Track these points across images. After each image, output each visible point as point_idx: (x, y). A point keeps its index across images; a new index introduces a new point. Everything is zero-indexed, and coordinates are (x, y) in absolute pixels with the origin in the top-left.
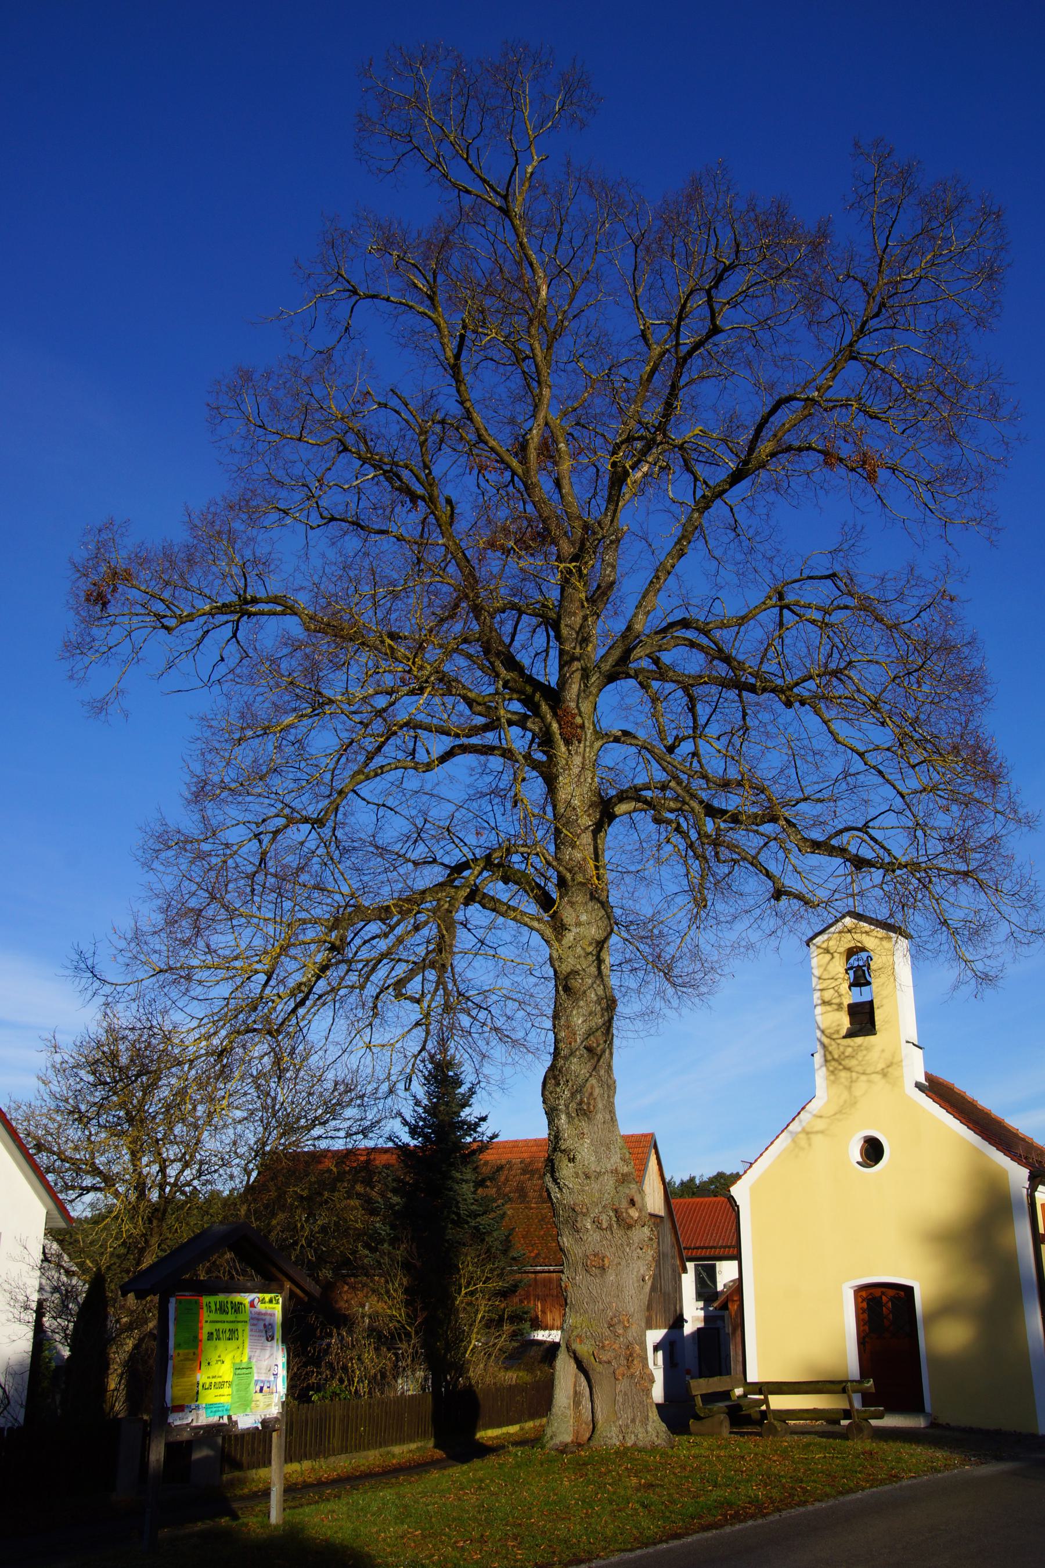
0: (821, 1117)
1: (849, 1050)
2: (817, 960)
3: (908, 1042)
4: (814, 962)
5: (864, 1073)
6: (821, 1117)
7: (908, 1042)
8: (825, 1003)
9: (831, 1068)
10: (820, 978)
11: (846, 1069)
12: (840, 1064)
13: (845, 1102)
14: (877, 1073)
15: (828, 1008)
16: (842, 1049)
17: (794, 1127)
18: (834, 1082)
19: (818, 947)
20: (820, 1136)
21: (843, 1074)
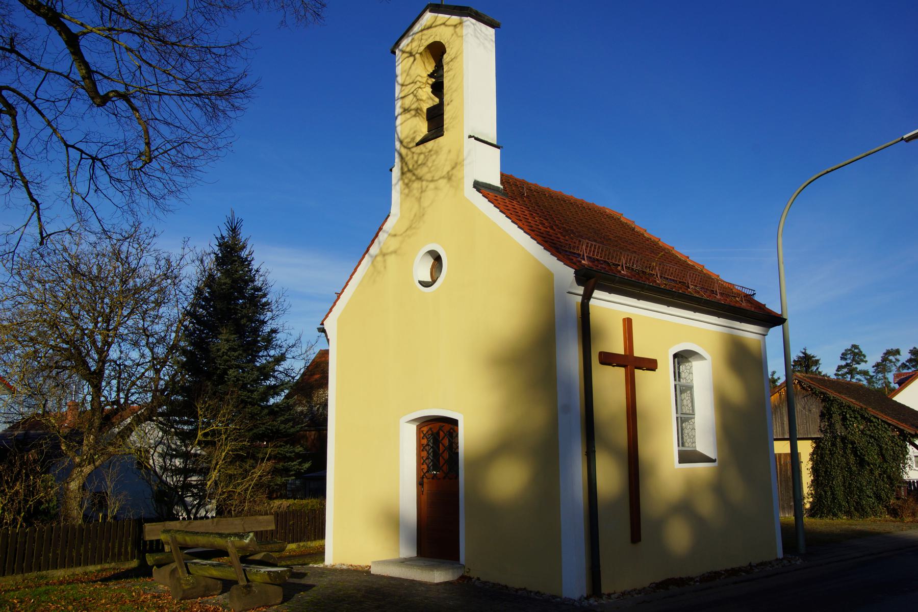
0: (395, 235)
1: (422, 156)
2: (402, 65)
3: (470, 137)
4: (399, 70)
5: (432, 181)
6: (395, 235)
7: (470, 137)
8: (406, 110)
9: (406, 181)
10: (402, 85)
11: (419, 179)
12: (414, 174)
13: (415, 215)
14: (443, 177)
15: (408, 115)
16: (415, 158)
17: (374, 250)
18: (407, 195)
19: (403, 52)
20: (393, 256)
21: (416, 185)
